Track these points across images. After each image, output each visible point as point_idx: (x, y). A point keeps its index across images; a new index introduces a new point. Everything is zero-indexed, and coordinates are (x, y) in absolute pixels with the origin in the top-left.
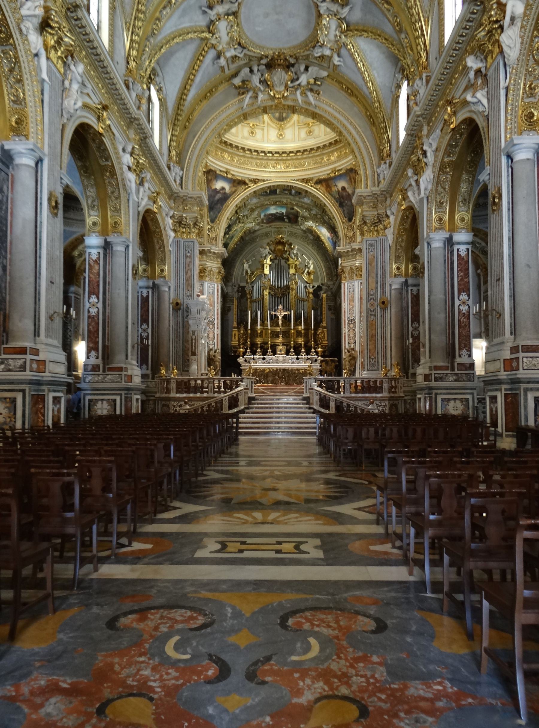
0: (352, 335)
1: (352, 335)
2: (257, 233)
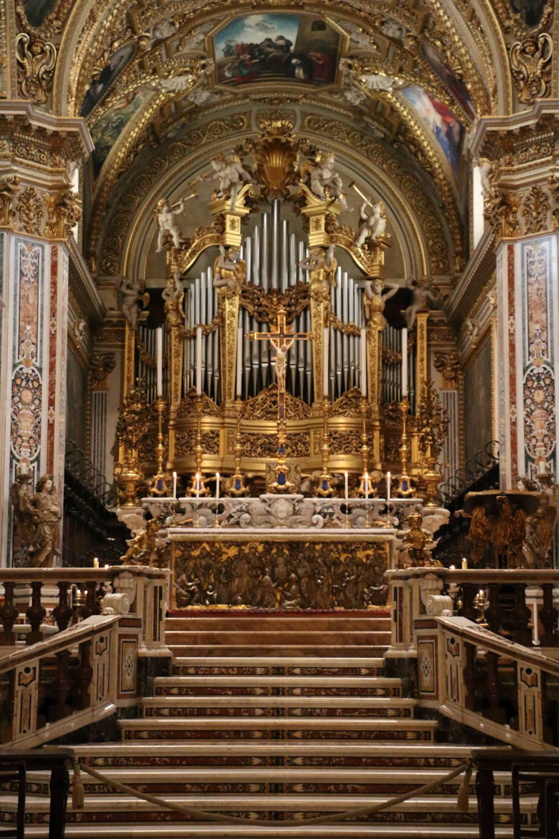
0: (539, 430)
1: (539, 430)
2: (202, 119)
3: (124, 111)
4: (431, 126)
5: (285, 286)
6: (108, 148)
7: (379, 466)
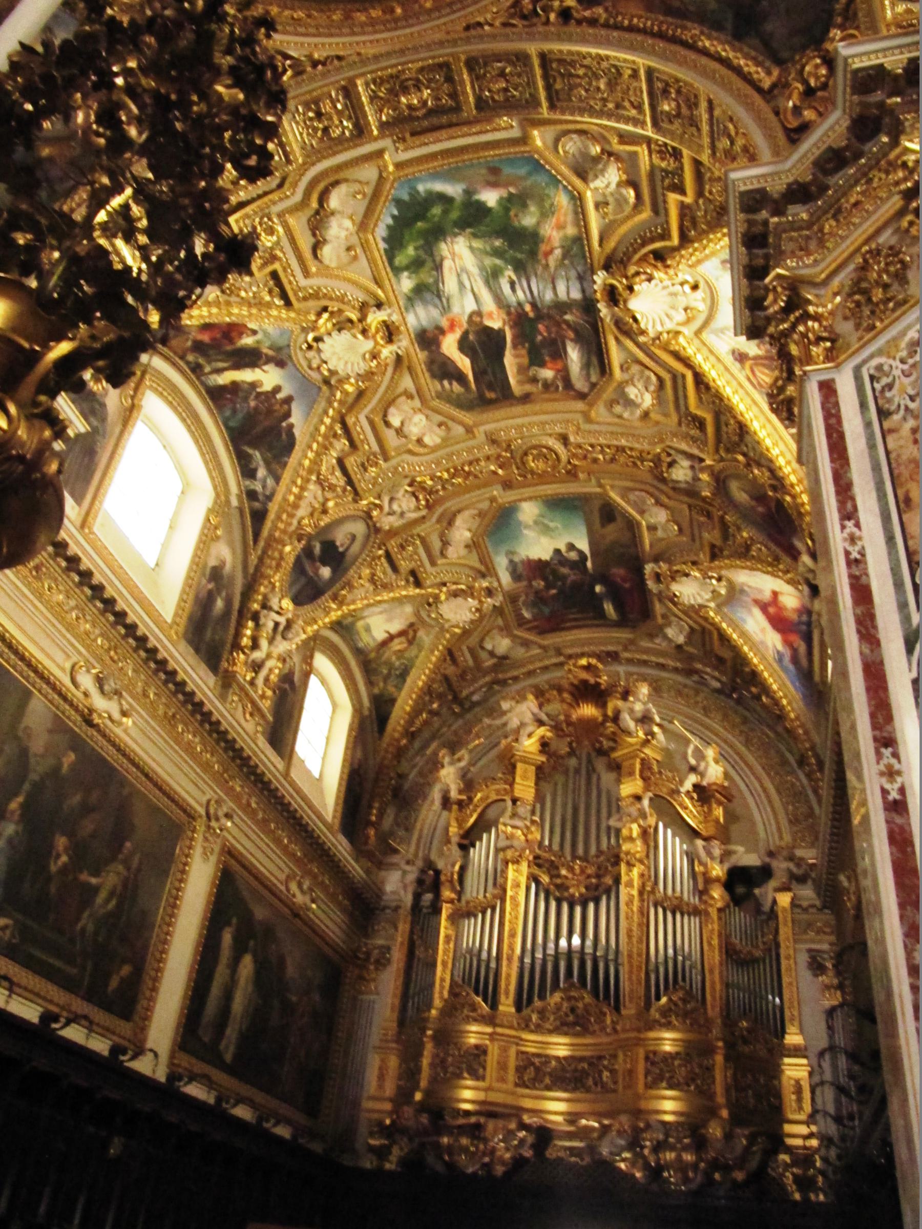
3: (407, 655)
4: (771, 652)
5: (593, 850)
6: (393, 701)
7: (725, 1113)
